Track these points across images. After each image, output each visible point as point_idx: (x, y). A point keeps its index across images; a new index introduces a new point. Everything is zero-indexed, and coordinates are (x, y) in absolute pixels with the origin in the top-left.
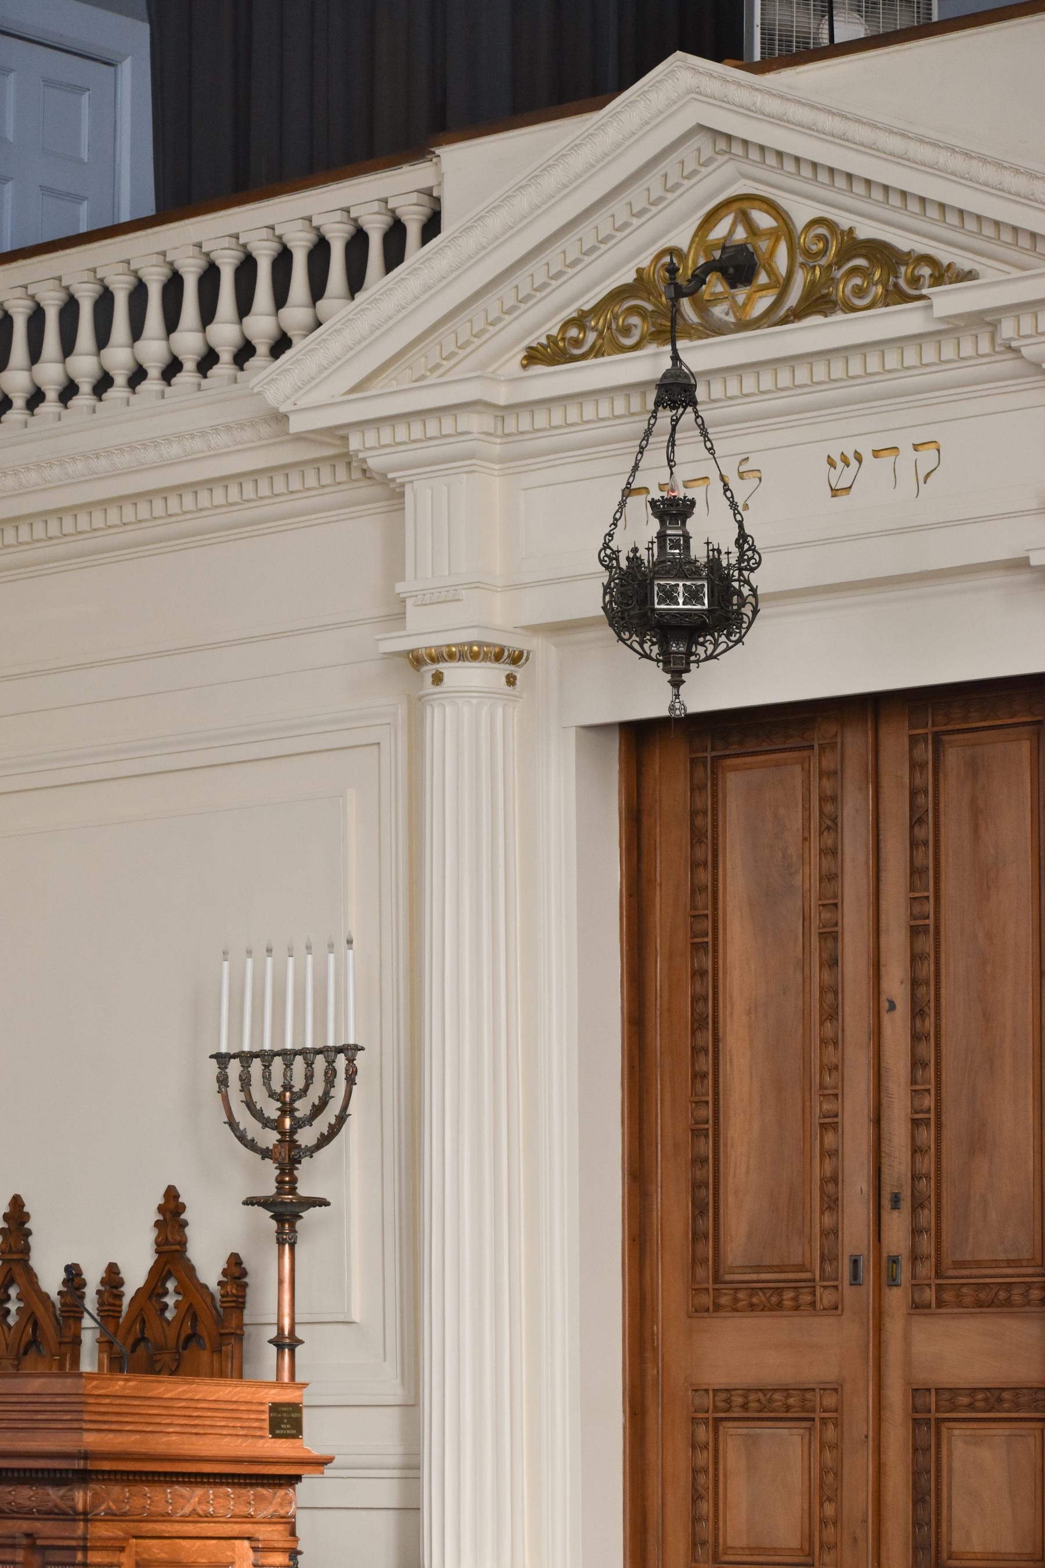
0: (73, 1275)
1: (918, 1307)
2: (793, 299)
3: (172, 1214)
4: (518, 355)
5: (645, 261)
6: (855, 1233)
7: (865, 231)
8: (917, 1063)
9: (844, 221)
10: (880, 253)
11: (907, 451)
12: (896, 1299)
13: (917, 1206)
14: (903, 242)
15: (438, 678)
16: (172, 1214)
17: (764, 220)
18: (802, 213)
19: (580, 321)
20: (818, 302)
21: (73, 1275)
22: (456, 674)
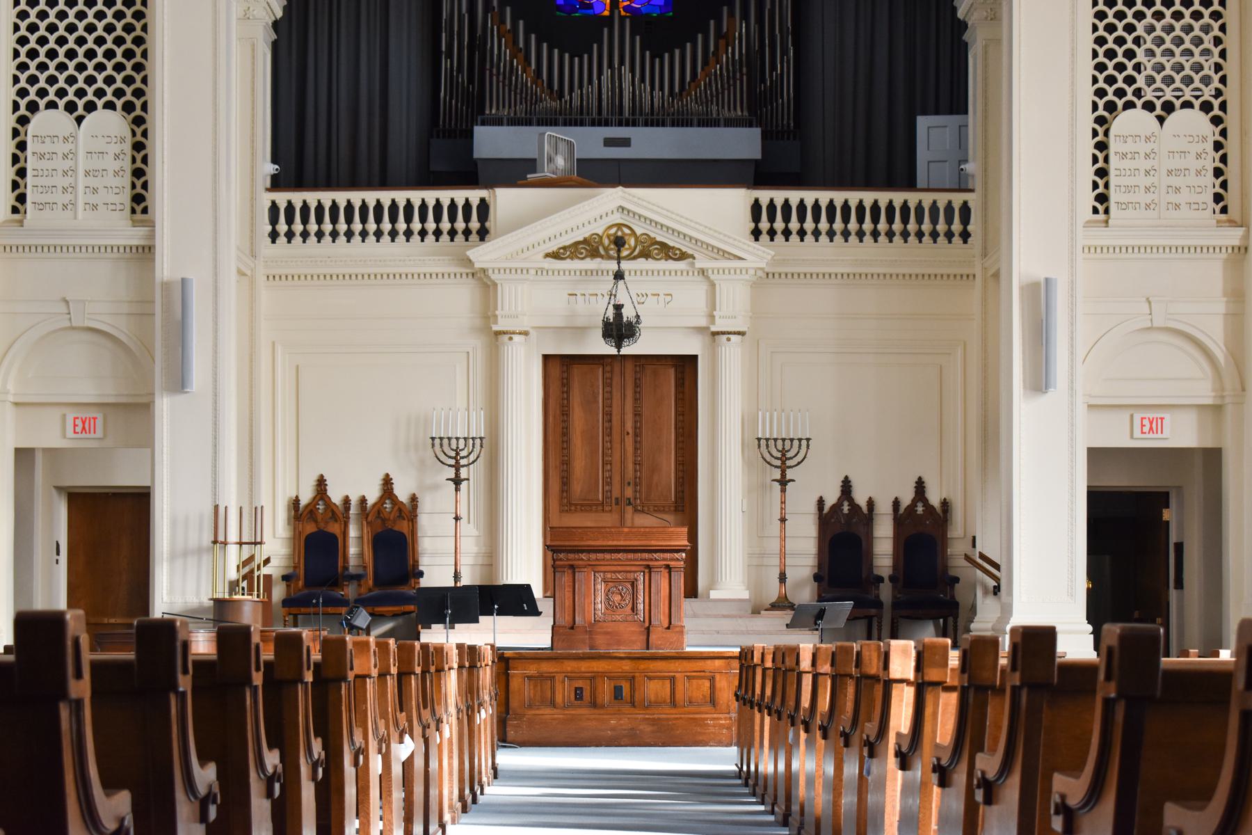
0: (347, 501)
1: (636, 510)
2: (636, 253)
3: (387, 482)
4: (542, 254)
5: (587, 235)
7: (659, 239)
8: (636, 449)
9: (653, 235)
11: (662, 297)
12: (630, 509)
13: (636, 485)
14: (671, 244)
15: (511, 339)
16: (387, 482)
17: (627, 231)
18: (639, 231)
19: (564, 248)
20: (645, 254)
21: (347, 501)
22: (516, 338)
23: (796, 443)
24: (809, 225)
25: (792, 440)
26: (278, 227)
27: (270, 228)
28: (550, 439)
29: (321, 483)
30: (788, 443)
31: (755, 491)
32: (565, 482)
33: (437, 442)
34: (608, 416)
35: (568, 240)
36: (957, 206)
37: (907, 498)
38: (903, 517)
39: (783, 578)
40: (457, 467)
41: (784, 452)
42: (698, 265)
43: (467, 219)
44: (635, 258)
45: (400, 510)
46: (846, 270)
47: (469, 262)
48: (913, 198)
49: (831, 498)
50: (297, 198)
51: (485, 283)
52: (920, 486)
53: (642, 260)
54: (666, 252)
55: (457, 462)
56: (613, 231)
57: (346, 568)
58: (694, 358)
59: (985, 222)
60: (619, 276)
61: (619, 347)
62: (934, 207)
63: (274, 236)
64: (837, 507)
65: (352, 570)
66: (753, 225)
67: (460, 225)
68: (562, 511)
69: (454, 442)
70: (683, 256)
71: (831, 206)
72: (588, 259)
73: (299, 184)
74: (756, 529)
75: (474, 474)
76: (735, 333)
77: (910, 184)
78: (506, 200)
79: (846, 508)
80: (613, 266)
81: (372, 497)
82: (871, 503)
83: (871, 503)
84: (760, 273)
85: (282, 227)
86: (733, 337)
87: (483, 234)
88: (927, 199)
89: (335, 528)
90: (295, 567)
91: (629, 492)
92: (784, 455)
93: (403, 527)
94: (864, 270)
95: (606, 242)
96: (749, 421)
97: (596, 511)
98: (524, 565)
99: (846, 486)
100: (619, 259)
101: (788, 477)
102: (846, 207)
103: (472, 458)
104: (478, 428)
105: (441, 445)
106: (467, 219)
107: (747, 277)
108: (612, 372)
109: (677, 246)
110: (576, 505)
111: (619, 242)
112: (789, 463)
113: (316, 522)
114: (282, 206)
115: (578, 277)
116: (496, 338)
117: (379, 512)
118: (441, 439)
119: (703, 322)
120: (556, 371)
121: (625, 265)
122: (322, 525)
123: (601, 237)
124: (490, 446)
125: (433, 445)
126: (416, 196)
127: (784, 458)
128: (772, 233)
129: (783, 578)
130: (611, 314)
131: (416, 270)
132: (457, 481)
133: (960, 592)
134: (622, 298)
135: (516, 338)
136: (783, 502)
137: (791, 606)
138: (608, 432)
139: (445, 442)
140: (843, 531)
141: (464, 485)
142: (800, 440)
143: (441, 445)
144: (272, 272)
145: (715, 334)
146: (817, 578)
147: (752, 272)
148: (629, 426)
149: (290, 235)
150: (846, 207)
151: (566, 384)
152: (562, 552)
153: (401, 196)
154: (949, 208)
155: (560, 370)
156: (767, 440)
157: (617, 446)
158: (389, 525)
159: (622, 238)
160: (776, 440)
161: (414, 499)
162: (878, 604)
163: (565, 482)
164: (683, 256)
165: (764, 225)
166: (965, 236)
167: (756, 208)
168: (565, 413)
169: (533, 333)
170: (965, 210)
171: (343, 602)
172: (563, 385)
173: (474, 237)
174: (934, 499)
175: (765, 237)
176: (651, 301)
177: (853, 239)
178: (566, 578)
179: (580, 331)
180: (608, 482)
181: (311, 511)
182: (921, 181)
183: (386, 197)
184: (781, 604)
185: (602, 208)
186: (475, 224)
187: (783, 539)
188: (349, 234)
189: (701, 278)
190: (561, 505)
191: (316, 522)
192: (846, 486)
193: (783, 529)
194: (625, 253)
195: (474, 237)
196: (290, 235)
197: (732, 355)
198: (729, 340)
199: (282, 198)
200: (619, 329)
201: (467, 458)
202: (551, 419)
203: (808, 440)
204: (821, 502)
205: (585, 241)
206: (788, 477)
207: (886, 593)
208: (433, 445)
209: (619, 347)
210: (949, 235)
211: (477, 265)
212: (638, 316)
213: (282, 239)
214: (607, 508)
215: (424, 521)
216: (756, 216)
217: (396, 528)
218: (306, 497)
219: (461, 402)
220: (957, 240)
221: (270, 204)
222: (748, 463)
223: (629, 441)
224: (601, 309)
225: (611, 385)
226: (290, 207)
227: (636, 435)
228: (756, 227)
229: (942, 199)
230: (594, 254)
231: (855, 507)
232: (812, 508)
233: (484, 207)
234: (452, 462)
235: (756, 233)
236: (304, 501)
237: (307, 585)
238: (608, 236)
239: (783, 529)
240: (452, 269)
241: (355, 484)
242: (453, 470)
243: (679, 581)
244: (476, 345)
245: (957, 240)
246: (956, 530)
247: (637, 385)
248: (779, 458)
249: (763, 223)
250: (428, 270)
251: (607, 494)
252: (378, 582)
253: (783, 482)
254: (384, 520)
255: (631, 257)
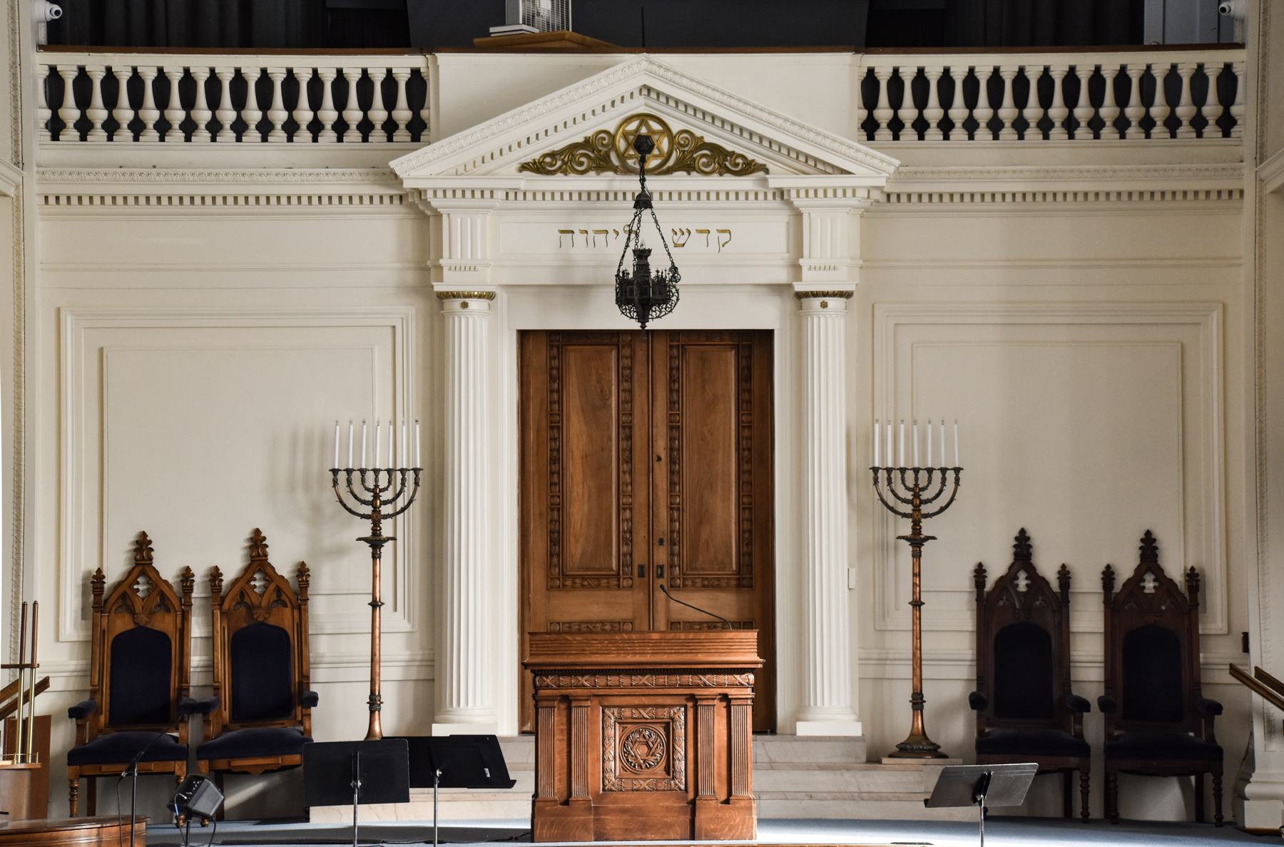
0: (187, 575)
2: (671, 163)
3: (257, 543)
4: (516, 165)
5: (589, 134)
6: (640, 557)
7: (709, 139)
8: (672, 484)
9: (698, 133)
10: (715, 148)
11: (714, 234)
13: (672, 543)
14: (729, 147)
15: (465, 305)
16: (257, 543)
17: (655, 126)
18: (675, 127)
19: (553, 155)
20: (686, 165)
21: (187, 575)
22: (474, 304)
23: (937, 476)
24: (958, 112)
25: (930, 471)
26: (62, 113)
27: (47, 114)
28: (531, 468)
29: (143, 546)
30: (923, 476)
31: (870, 553)
32: (556, 539)
33: (342, 476)
34: (626, 429)
35: (558, 142)
36: (1212, 74)
37: (1126, 568)
38: (1120, 600)
39: (918, 701)
40: (376, 518)
41: (917, 490)
42: (777, 180)
43: (390, 104)
44: (669, 171)
45: (279, 590)
46: (1019, 187)
47: (394, 178)
48: (1135, 62)
49: (997, 568)
50: (96, 63)
51: (422, 213)
52: (1149, 546)
53: (681, 174)
54: (723, 161)
55: (376, 510)
56: (633, 126)
57: (183, 689)
58: (768, 335)
59: (1262, 101)
60: (643, 202)
61: (643, 318)
62: (1173, 76)
63: (56, 127)
64: (1007, 582)
65: (193, 694)
66: (864, 113)
67: (378, 114)
68: (550, 588)
69: (370, 476)
70: (749, 168)
71: (996, 79)
72: (592, 173)
73: (99, 40)
74: (871, 618)
75: (404, 530)
76: (834, 294)
77: (1133, 39)
78: (456, 74)
79: (1022, 583)
80: (631, 184)
81: (232, 568)
82: (1065, 575)
83: (1065, 575)
84: (876, 195)
85: (71, 113)
86: (831, 302)
87: (417, 129)
88: (1161, 62)
89: (165, 624)
90: (93, 692)
91: (661, 556)
92: (916, 496)
93: (285, 618)
94: (1049, 187)
95: (622, 145)
96: (858, 440)
97: (608, 587)
98: (486, 701)
99: (1023, 547)
100: (643, 173)
101: (925, 532)
102: (1021, 80)
103: (400, 503)
104: (411, 454)
105: (349, 482)
106: (390, 104)
107: (855, 202)
108: (632, 357)
109: (739, 150)
110: (574, 577)
111: (643, 145)
112: (925, 509)
113: (132, 612)
114: (69, 77)
115: (575, 203)
116: (439, 304)
117: (242, 594)
118: (349, 471)
119: (782, 276)
120: (540, 357)
121: (653, 184)
122: (143, 619)
123: (613, 137)
124: (433, 482)
125: (335, 482)
126: (303, 64)
127: (917, 500)
128: (896, 126)
129: (918, 701)
130: (629, 265)
131: (305, 190)
132: (376, 542)
133: (1224, 728)
134: (649, 238)
135: (474, 304)
136: (917, 575)
137: (934, 751)
138: (627, 457)
139: (356, 476)
140: (1018, 618)
141: (387, 549)
142: (944, 470)
143: (349, 482)
144: (53, 190)
145: (801, 296)
146: (976, 701)
147: (862, 193)
148: (661, 446)
149: (84, 127)
150: (1021, 80)
151: (556, 378)
152: (550, 676)
153: (277, 64)
154: (1199, 76)
155: (548, 357)
156: (889, 470)
157: (640, 479)
158: (260, 616)
159: (647, 138)
160: (903, 470)
161: (302, 571)
162: (1082, 749)
163: (556, 539)
164: (749, 168)
165: (883, 113)
166: (1227, 123)
167: (870, 83)
168: (556, 425)
169: (502, 297)
170: (1228, 78)
171: (177, 752)
172: (552, 379)
173: (402, 135)
174: (1174, 568)
175: (884, 134)
176: (696, 241)
177: (1032, 133)
178: (557, 719)
179: (579, 292)
180: (627, 538)
181: (124, 596)
182: (1151, 31)
183: (251, 64)
184: (918, 746)
185: (613, 88)
186: (403, 114)
187: (917, 635)
188: (189, 128)
189: (778, 203)
190: (550, 577)
191: (132, 612)
192: (1023, 547)
193: (917, 620)
194: (652, 163)
195: (402, 135)
196: (84, 127)
197: (830, 331)
198: (824, 305)
199: (68, 63)
200: (644, 290)
201: (397, 502)
202: (532, 436)
203: (957, 470)
204: (980, 572)
205: (587, 143)
206: (925, 532)
207: (1094, 728)
208: (335, 482)
209: (643, 318)
210: (1199, 123)
211: (408, 184)
212: (674, 269)
213: (71, 134)
214: (625, 583)
215: (320, 608)
216: (870, 98)
217: (272, 621)
218: (115, 570)
219: (382, 411)
220: (1211, 130)
221: (46, 72)
222: (857, 509)
223: (661, 471)
224: (612, 256)
225: (630, 379)
226: (83, 78)
227: (672, 461)
228: (870, 116)
229: (1187, 62)
230: (602, 164)
231: (1037, 582)
232: (965, 582)
233: (418, 83)
234: (368, 510)
235: (870, 127)
236: (113, 576)
237: (113, 721)
238: (625, 135)
239: (917, 620)
240: (367, 190)
241: (200, 547)
242: (368, 524)
243: (745, 717)
244: (407, 315)
245: (1211, 130)
246: (1214, 622)
247: (674, 379)
248: (910, 500)
249: (880, 113)
250: (325, 190)
251: (626, 560)
252: (238, 713)
253: (917, 541)
254: (251, 608)
255: (661, 171)
